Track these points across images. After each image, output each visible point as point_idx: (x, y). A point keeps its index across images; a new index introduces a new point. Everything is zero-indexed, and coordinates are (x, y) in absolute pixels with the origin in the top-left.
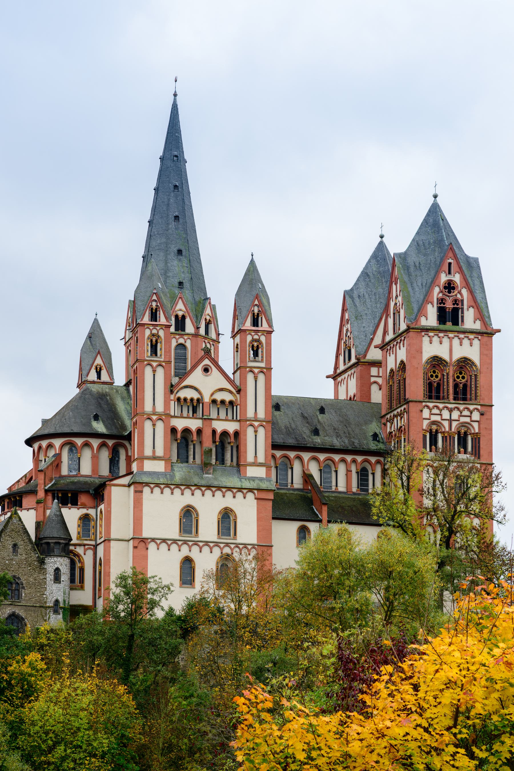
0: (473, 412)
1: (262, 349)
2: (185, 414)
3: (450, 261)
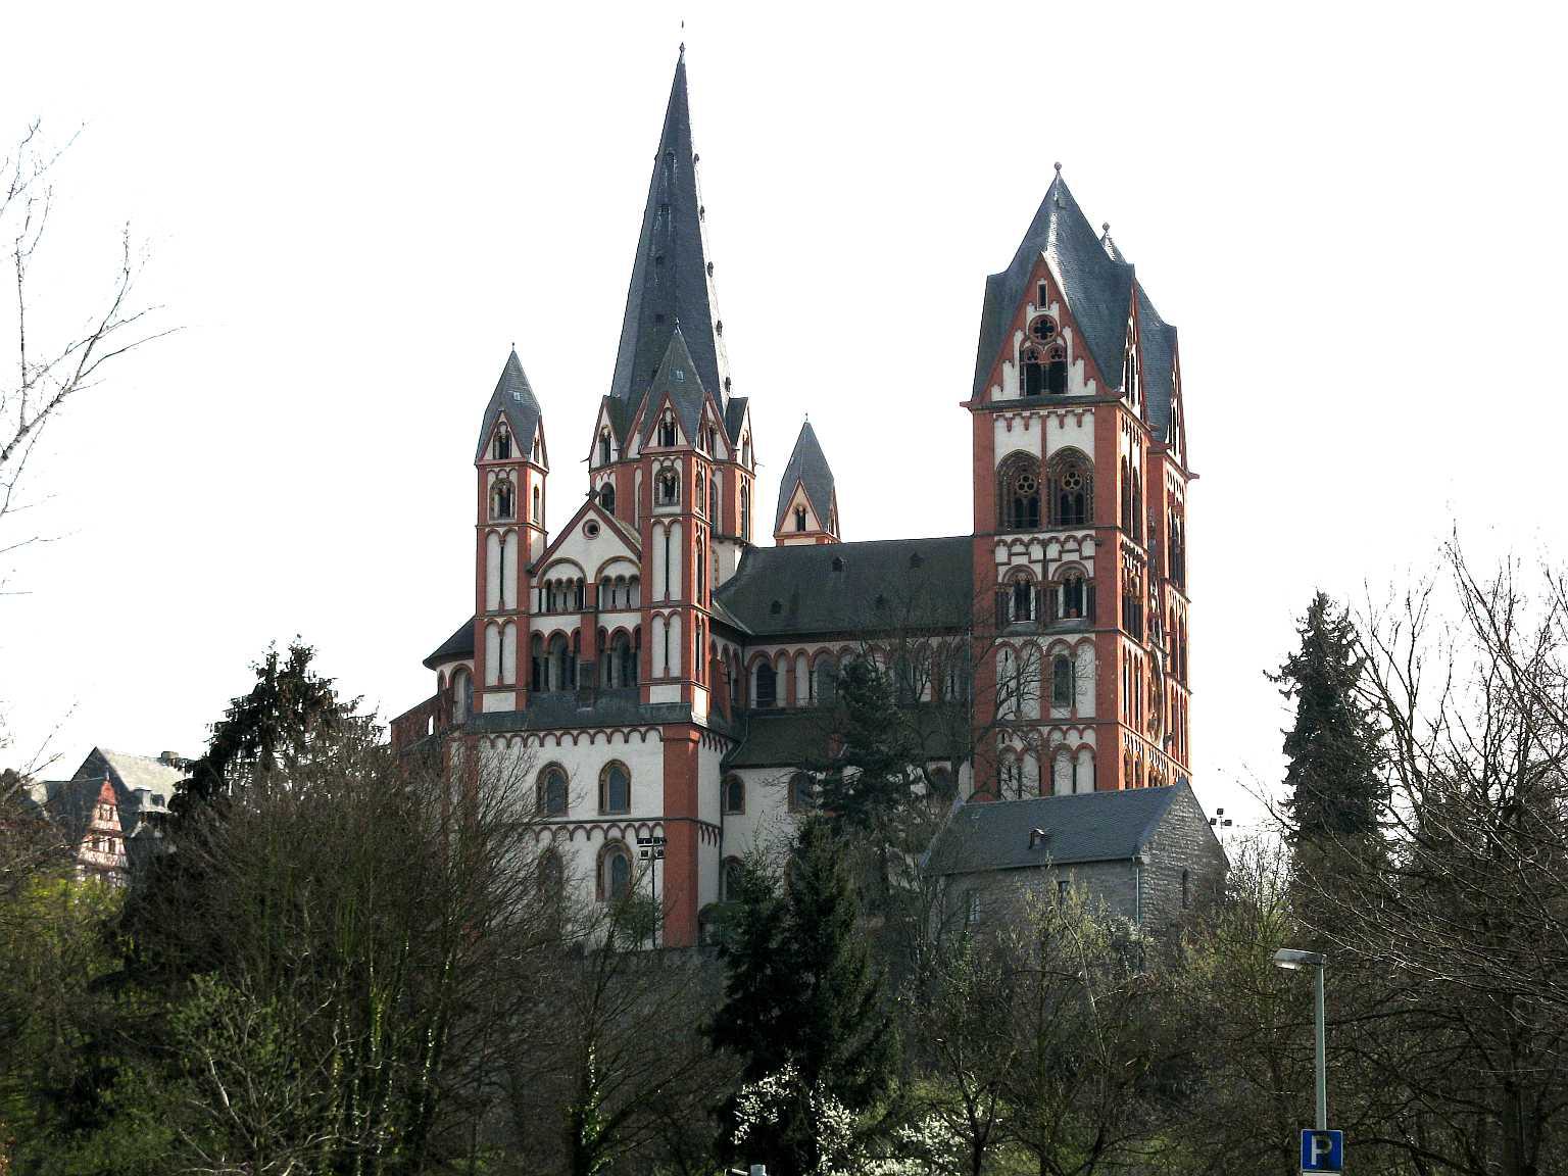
0: (1084, 543)
3: (1042, 282)
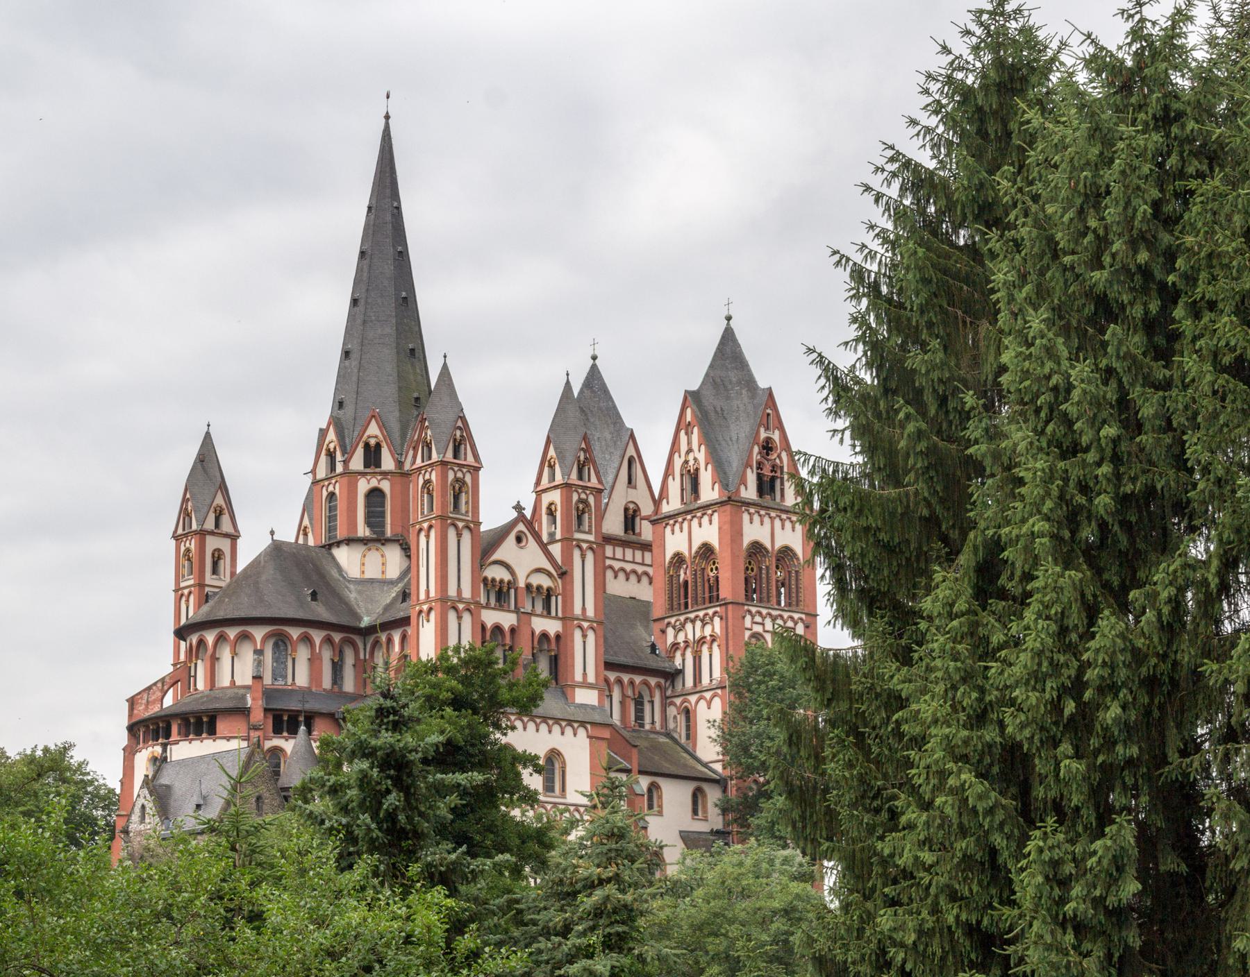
1: (590, 515)
2: (493, 602)
